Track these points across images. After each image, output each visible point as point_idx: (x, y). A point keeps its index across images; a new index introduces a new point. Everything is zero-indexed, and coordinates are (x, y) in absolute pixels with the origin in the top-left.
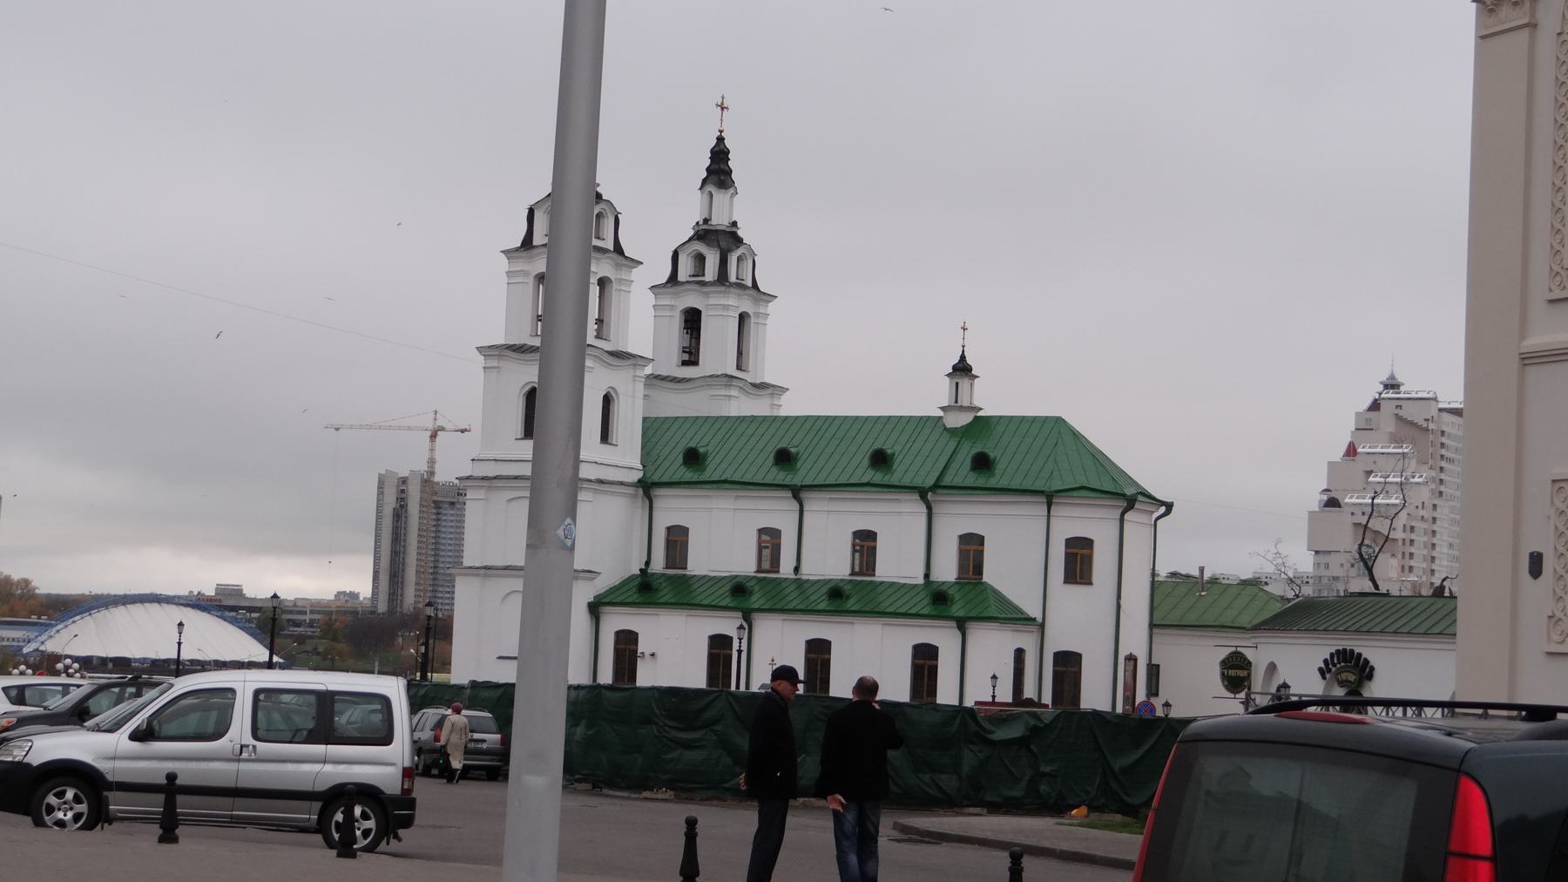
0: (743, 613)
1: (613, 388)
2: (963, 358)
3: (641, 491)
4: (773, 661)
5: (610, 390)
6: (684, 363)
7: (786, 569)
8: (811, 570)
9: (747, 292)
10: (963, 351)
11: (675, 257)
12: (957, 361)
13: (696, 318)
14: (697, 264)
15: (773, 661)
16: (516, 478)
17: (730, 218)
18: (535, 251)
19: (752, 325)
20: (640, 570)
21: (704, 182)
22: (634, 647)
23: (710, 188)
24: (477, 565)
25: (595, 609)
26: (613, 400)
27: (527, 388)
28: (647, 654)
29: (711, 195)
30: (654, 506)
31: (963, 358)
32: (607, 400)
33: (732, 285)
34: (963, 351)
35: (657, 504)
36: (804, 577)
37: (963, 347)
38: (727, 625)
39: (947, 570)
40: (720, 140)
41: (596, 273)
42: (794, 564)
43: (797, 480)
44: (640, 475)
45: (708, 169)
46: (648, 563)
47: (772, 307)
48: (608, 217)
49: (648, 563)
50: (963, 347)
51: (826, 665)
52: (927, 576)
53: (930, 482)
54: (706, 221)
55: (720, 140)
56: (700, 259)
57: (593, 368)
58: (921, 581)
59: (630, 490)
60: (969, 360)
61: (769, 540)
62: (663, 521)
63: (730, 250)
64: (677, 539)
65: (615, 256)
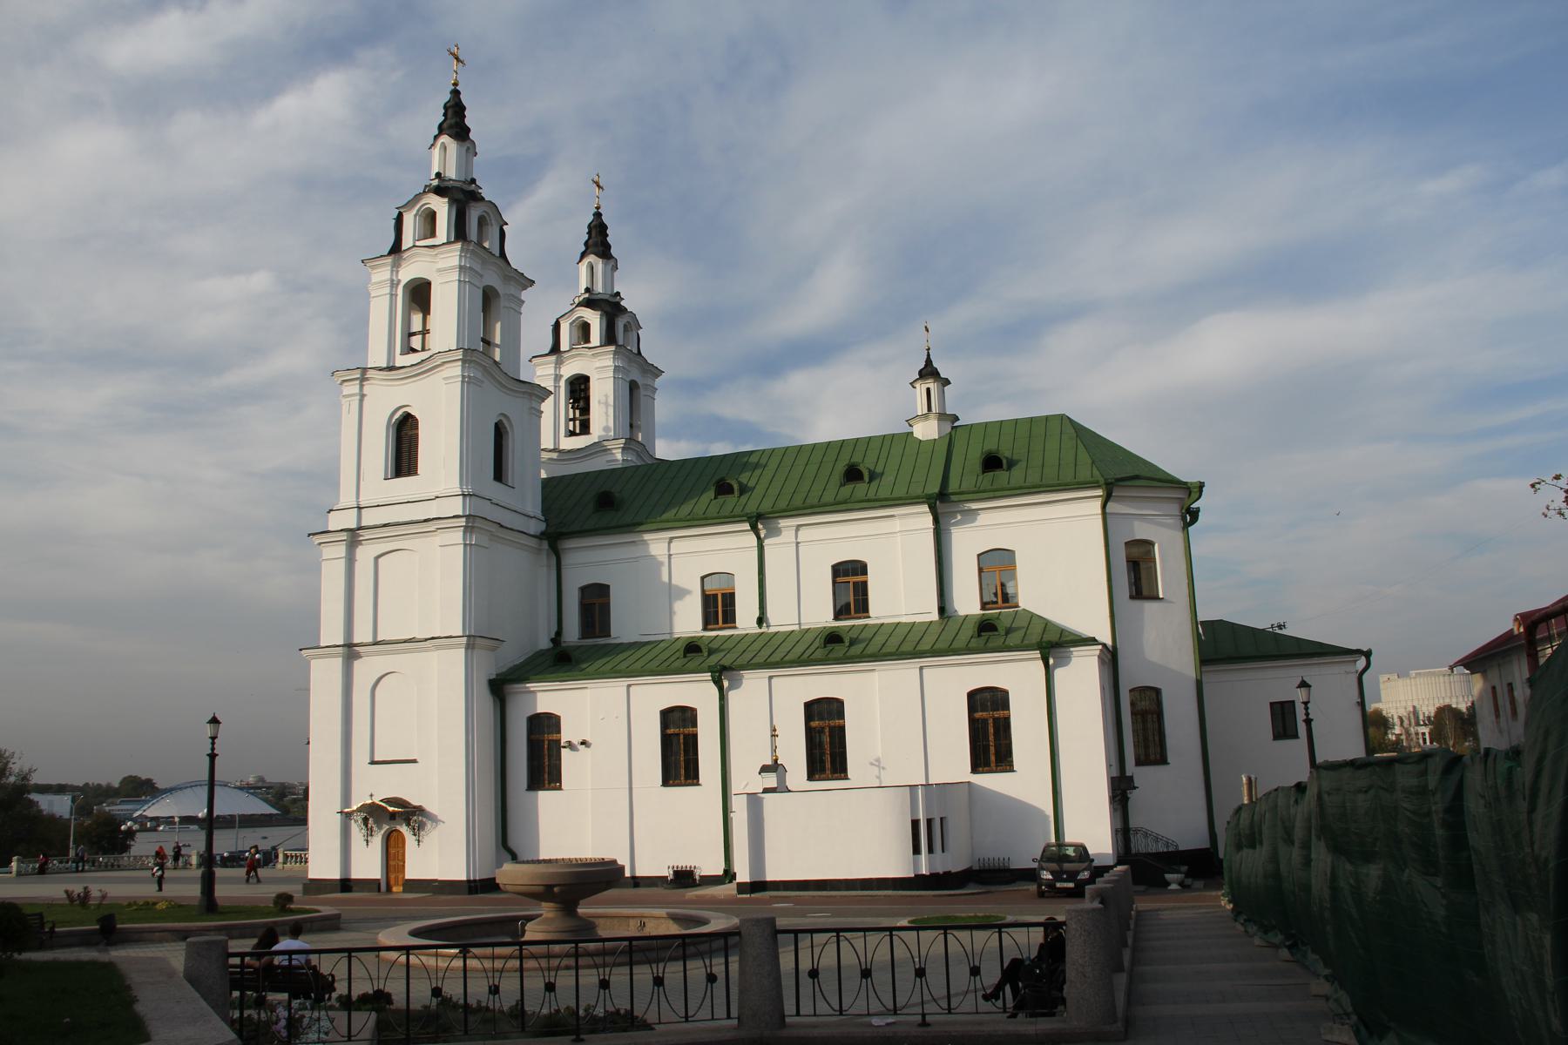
1: (502, 414)
2: (929, 362)
3: (545, 545)
5: (505, 421)
6: (572, 434)
7: (746, 619)
8: (782, 619)
10: (928, 355)
11: (556, 328)
12: (923, 366)
14: (580, 335)
16: (385, 525)
17: (613, 288)
18: (405, 255)
19: (642, 398)
20: (552, 640)
21: (583, 255)
22: (554, 737)
23: (591, 258)
24: (338, 644)
25: (500, 688)
26: (507, 432)
27: (397, 416)
28: (575, 741)
30: (563, 563)
31: (929, 362)
32: (500, 433)
33: (621, 346)
34: (928, 355)
35: (569, 560)
36: (772, 630)
38: (696, 692)
39: (967, 602)
40: (598, 215)
41: (481, 276)
43: (752, 508)
44: (543, 527)
45: (586, 244)
46: (559, 633)
47: (658, 382)
48: (492, 225)
49: (559, 633)
50: (928, 349)
53: (934, 488)
54: (587, 290)
55: (598, 215)
56: (585, 329)
57: (482, 382)
58: (934, 616)
59: (533, 542)
64: (596, 601)
65: (501, 262)
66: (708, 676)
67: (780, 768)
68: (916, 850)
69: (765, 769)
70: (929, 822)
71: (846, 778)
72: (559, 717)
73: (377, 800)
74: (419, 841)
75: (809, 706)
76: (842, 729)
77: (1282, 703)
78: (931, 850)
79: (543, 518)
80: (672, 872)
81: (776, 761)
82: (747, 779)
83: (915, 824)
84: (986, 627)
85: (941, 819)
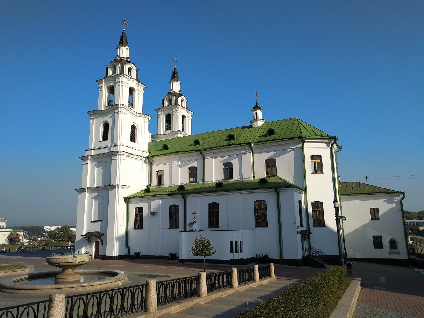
0: (182, 195)
2: (257, 104)
4: (194, 212)
9: (184, 109)
10: (257, 102)
13: (169, 117)
15: (194, 212)
19: (187, 120)
20: (147, 186)
29: (173, 84)
31: (257, 104)
34: (257, 102)
37: (257, 101)
41: (128, 84)
42: (202, 178)
48: (133, 70)
51: (217, 213)
52: (254, 177)
60: (259, 105)
61: (193, 171)
62: (156, 168)
63: (179, 97)
66: (181, 196)
67: (195, 224)
68: (232, 251)
69: (192, 224)
70: (236, 242)
71: (219, 227)
72: (143, 208)
73: (90, 232)
74: (103, 244)
75: (209, 205)
76: (218, 212)
77: (374, 208)
78: (236, 251)
79: (148, 152)
80: (170, 255)
81: (194, 221)
82: (188, 228)
83: (231, 243)
84: (263, 181)
85: (241, 242)
